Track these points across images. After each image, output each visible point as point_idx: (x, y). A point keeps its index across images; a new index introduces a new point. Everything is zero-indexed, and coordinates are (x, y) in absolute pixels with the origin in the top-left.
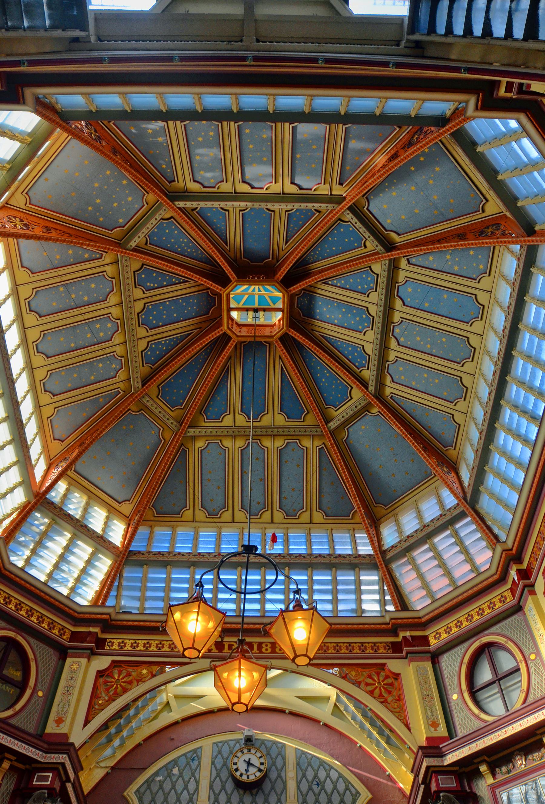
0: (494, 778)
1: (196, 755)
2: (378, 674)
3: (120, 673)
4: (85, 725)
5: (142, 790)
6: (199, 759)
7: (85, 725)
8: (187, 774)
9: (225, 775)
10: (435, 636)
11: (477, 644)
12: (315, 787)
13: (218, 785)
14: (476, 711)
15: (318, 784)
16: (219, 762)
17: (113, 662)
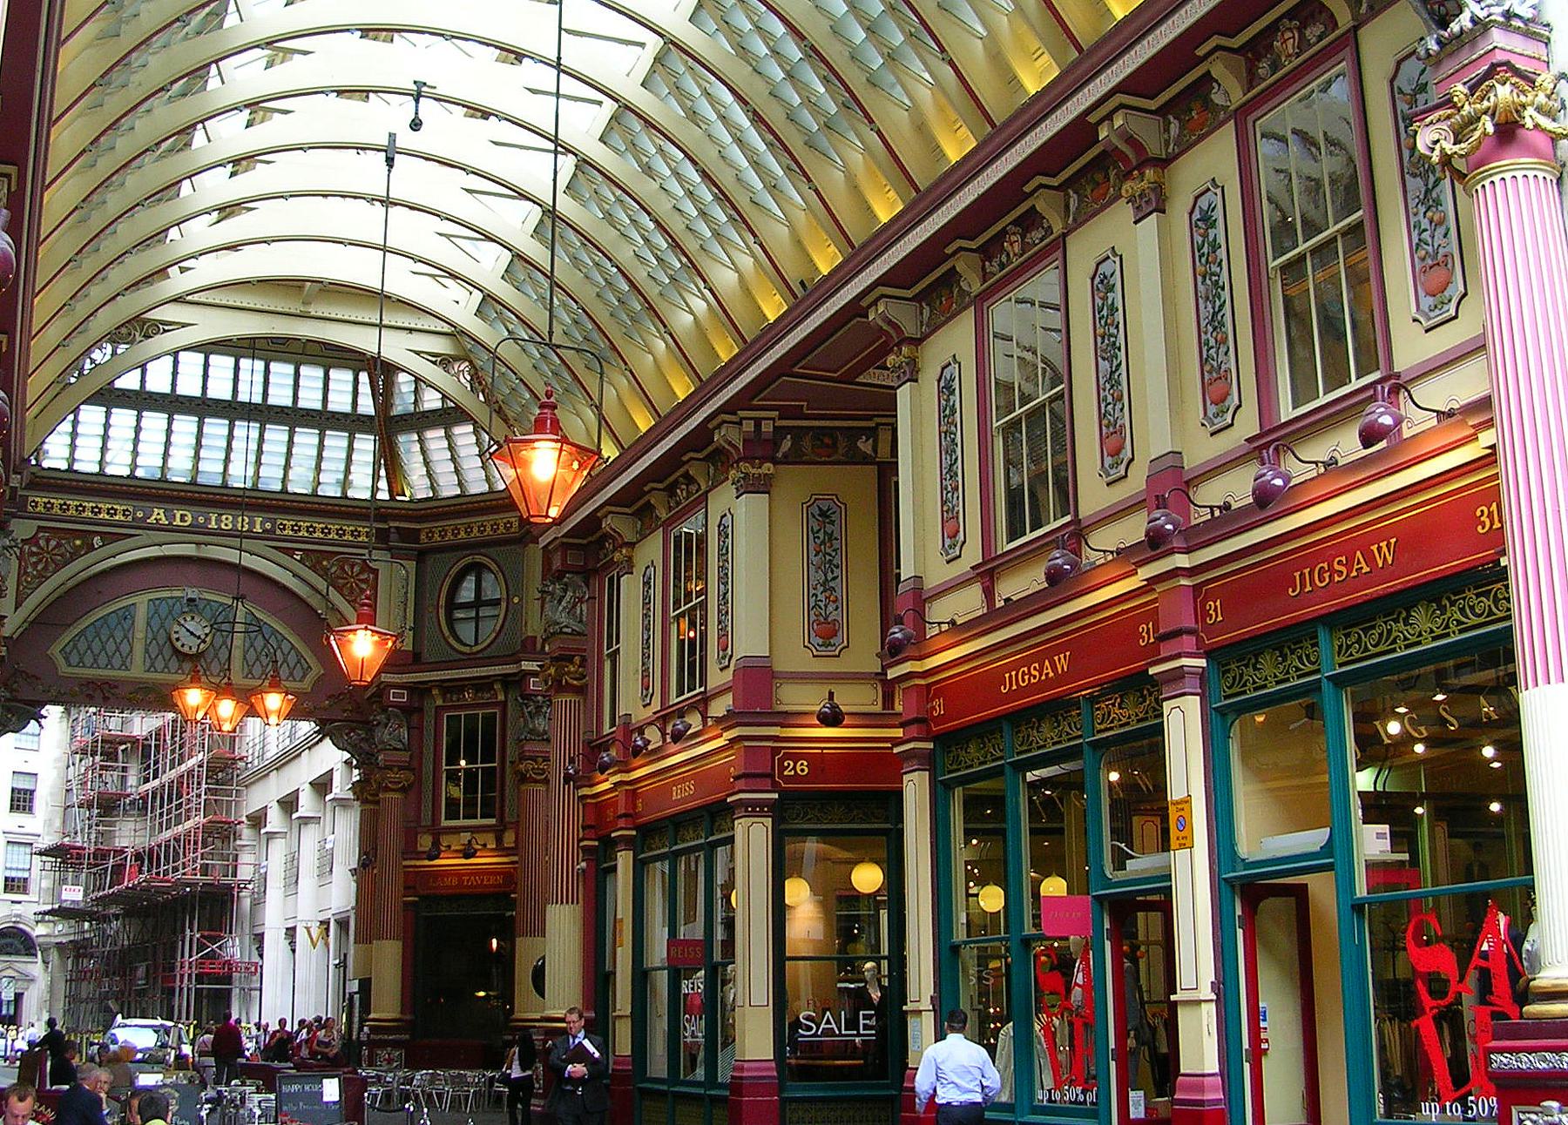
0: (444, 702)
1: (127, 614)
2: (352, 567)
3: (48, 541)
4: (16, 608)
5: (68, 650)
6: (133, 618)
7: (16, 608)
8: (119, 635)
9: (162, 639)
10: (427, 534)
11: (468, 560)
12: (263, 658)
13: (154, 650)
14: (447, 633)
15: (267, 656)
16: (156, 623)
17: (40, 528)
